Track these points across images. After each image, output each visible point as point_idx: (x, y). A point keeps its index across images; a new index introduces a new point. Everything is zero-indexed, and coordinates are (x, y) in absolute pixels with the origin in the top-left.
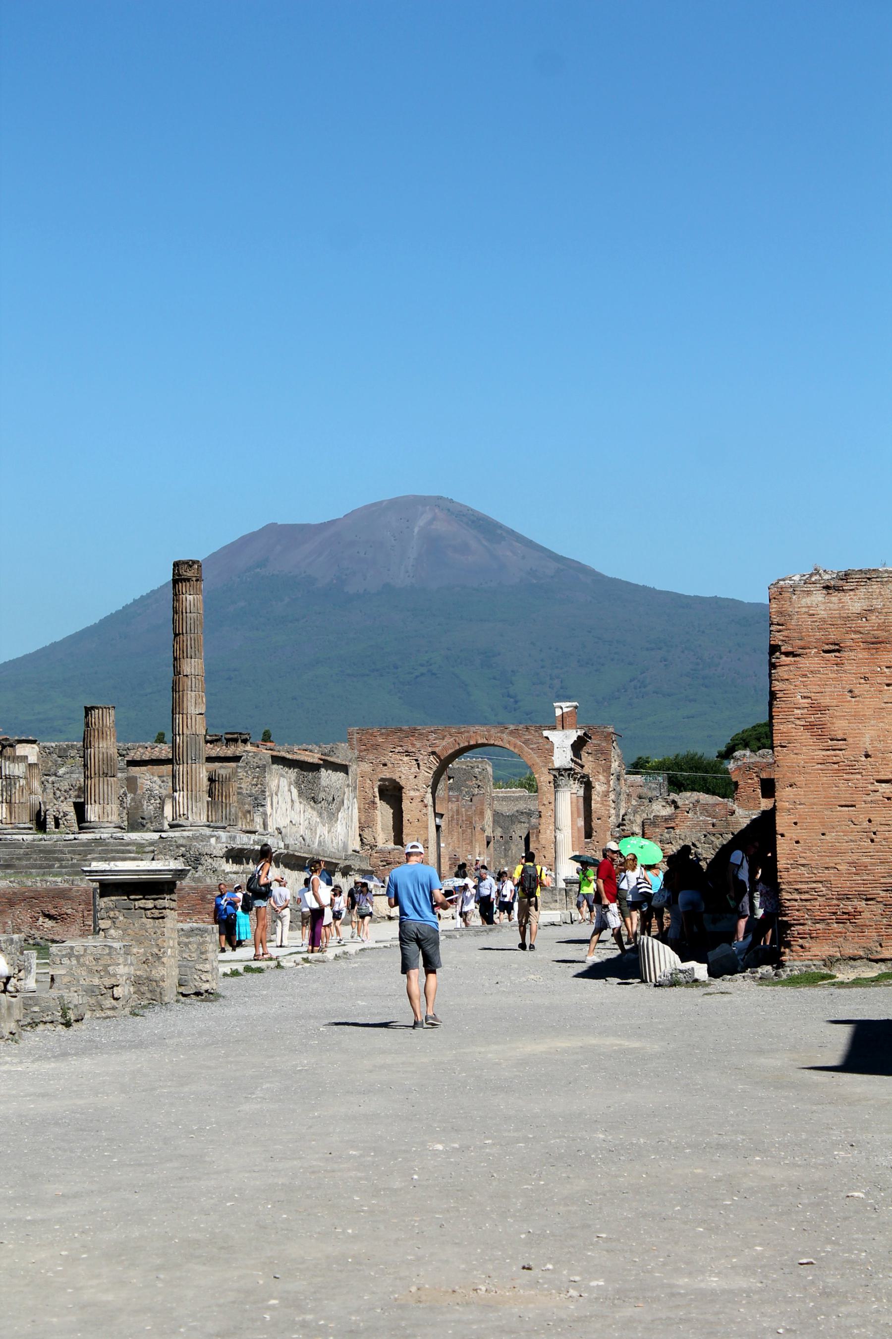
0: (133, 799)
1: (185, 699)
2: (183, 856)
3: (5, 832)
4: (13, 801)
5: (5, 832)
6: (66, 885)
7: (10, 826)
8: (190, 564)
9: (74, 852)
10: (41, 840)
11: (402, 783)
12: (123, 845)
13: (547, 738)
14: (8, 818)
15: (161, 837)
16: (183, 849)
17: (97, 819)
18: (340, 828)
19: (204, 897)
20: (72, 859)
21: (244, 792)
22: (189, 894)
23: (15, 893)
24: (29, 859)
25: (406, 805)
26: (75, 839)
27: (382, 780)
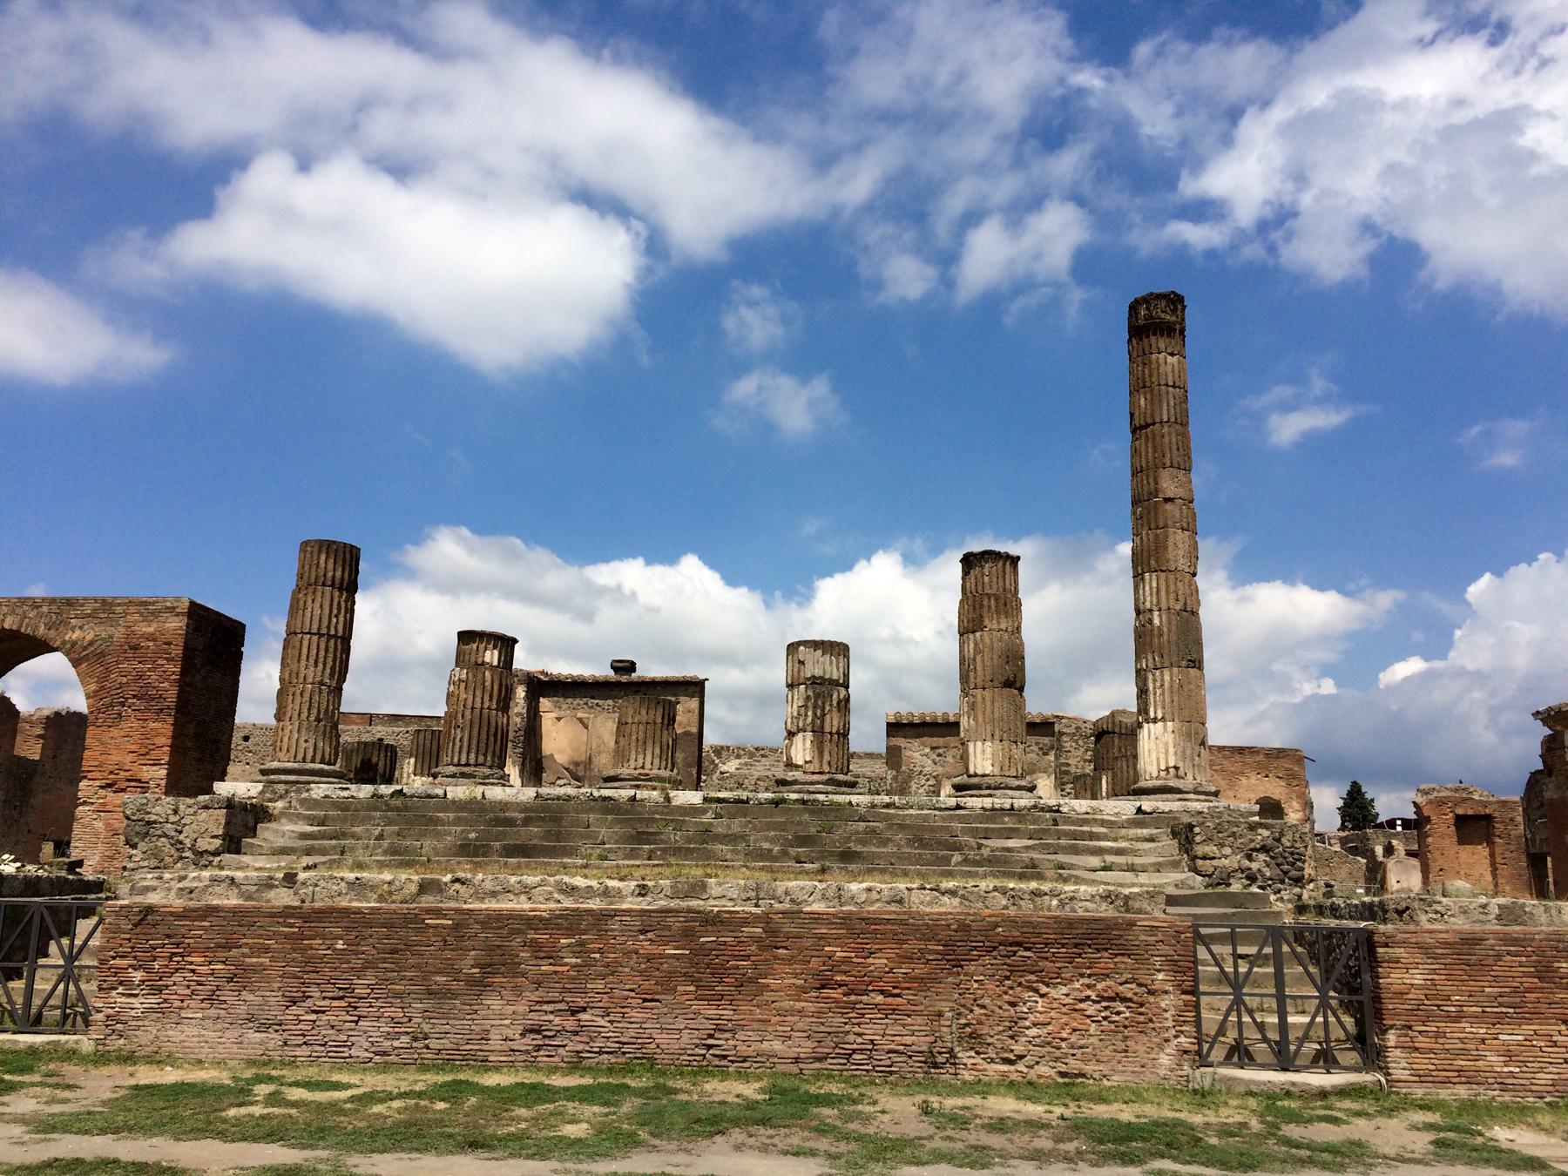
0: (895, 778)
1: (1170, 543)
2: (1264, 849)
3: (812, 788)
4: (827, 729)
5: (812, 788)
6: (1106, 911)
7: (816, 777)
8: (1175, 301)
9: (974, 832)
10: (888, 806)
12: (1073, 823)
14: (816, 760)
15: (1139, 810)
16: (1266, 833)
17: (997, 772)
19: (1549, 969)
20: (980, 846)
21: (1073, 770)
22: (1499, 957)
23: (964, 927)
26: (958, 807)
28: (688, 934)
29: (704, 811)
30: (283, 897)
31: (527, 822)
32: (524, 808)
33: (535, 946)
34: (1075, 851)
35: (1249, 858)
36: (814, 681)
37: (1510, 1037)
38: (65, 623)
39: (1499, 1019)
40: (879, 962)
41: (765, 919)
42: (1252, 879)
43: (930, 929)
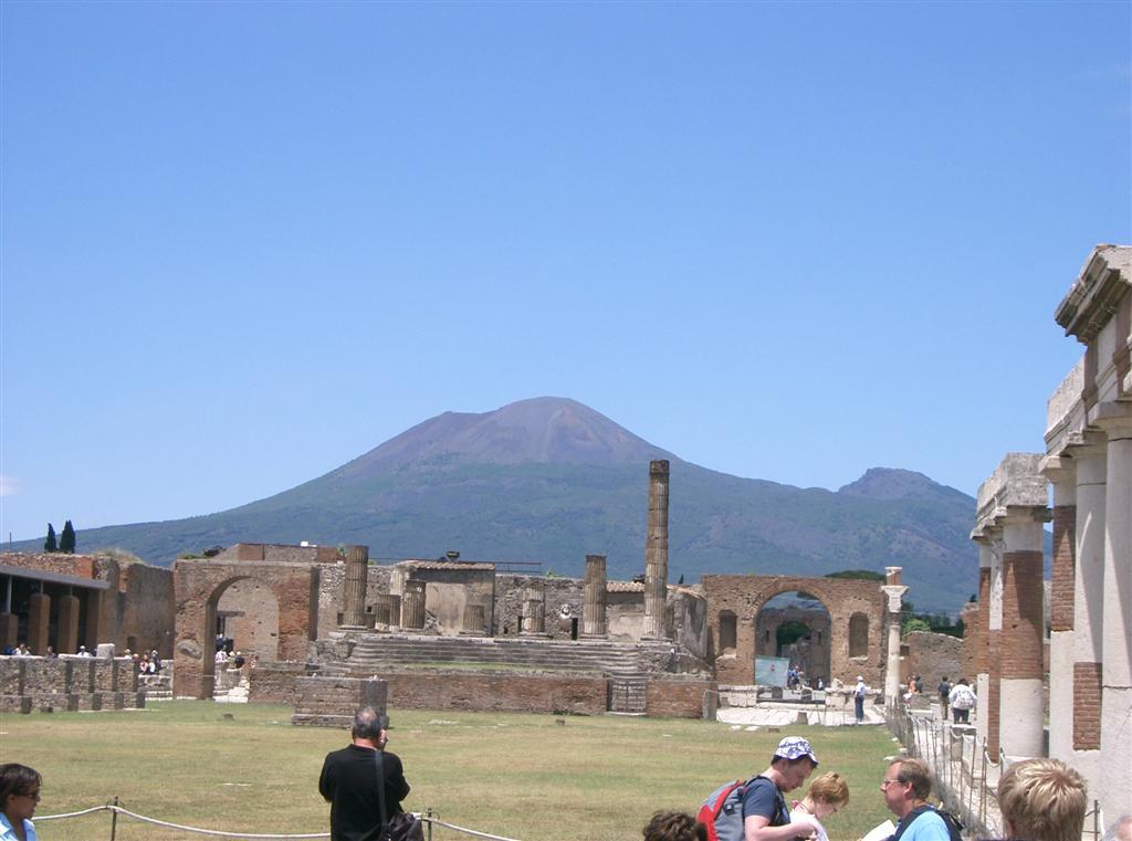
6: (590, 677)
11: (738, 614)
13: (884, 592)
18: (700, 643)
24: (552, 657)
25: (739, 627)
27: (722, 611)
28: (490, 682)
29: (494, 646)
30: (389, 672)
31: (437, 649)
32: (435, 643)
33: (453, 685)
34: (608, 660)
35: (653, 662)
36: (532, 601)
37: (674, 705)
38: (267, 573)
39: (671, 701)
40: (535, 688)
41: (508, 679)
42: (654, 669)
43: (548, 681)
